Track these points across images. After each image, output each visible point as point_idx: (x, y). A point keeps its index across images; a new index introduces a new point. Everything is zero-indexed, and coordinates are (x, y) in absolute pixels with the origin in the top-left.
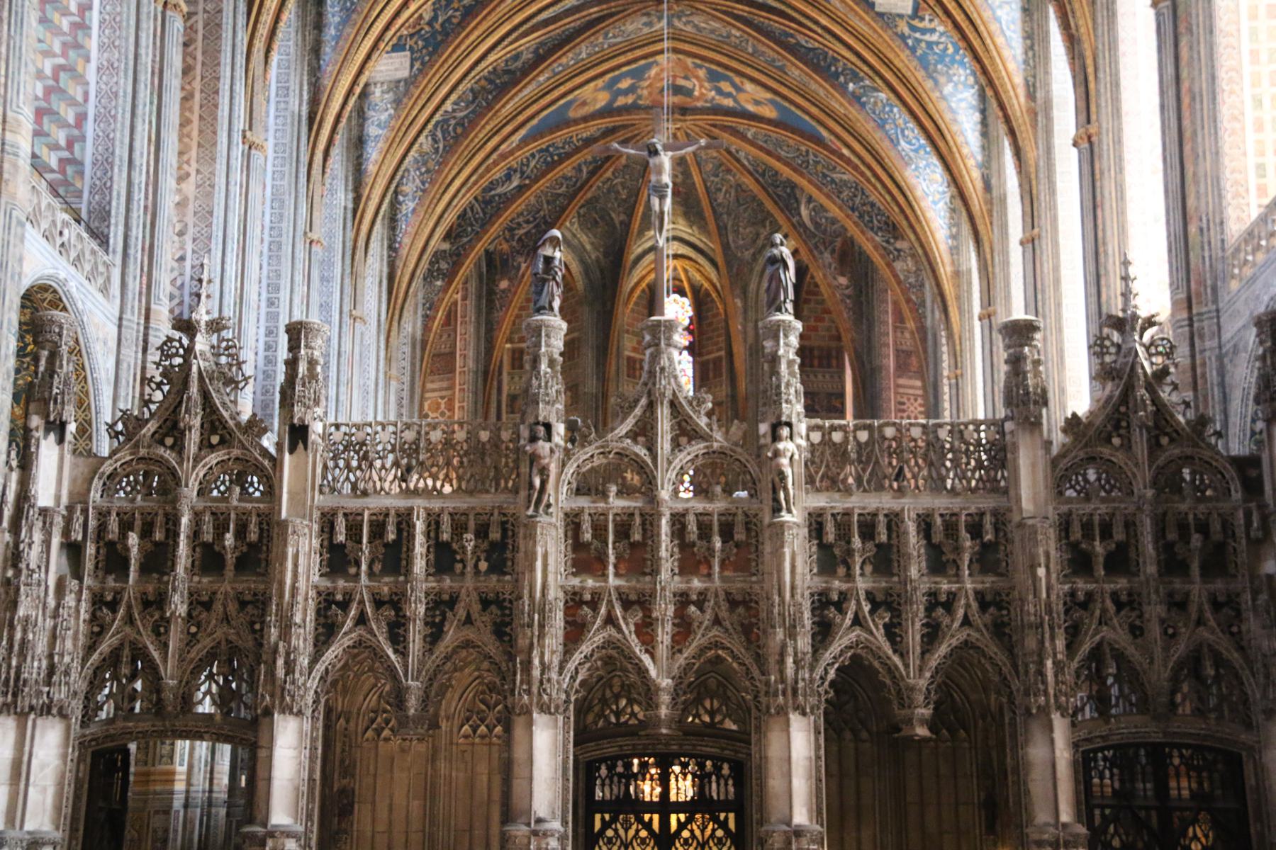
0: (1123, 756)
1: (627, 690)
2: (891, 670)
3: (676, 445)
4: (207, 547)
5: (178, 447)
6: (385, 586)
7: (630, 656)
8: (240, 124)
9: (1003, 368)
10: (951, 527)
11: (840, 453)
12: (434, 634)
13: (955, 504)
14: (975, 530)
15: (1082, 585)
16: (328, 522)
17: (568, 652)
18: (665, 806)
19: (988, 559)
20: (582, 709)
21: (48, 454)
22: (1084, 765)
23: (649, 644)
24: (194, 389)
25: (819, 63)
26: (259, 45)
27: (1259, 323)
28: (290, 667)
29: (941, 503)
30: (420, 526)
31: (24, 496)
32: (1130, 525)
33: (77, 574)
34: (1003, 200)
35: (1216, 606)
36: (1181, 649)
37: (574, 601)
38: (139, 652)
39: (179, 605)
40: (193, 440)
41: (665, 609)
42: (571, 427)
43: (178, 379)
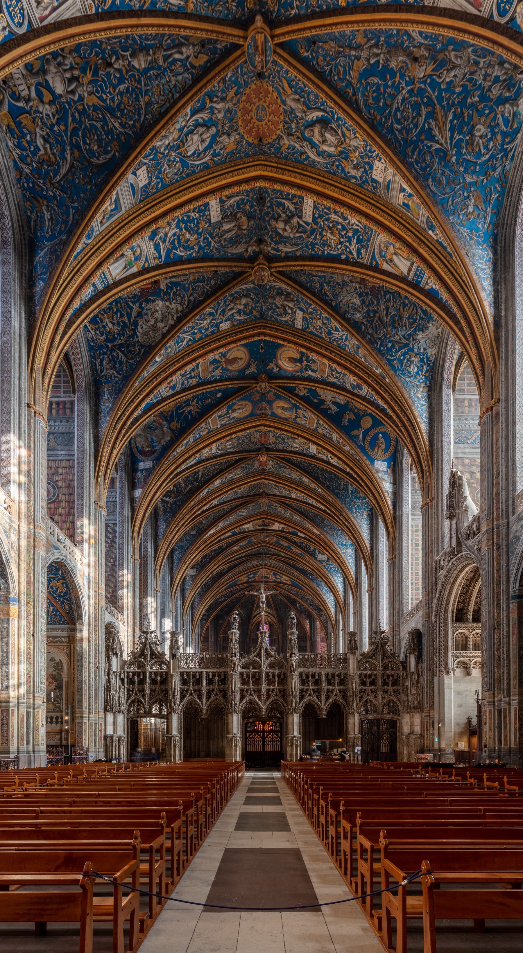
0: (371, 722)
1: (255, 709)
2: (318, 705)
3: (267, 658)
4: (153, 680)
5: (145, 658)
6: (196, 687)
7: (256, 702)
8: (154, 586)
9: (347, 642)
10: (333, 675)
11: (307, 660)
13: (334, 671)
14: (339, 676)
15: (364, 688)
16: (182, 674)
17: (241, 701)
18: (263, 731)
19: (342, 682)
20: (244, 712)
21: (114, 660)
22: (362, 723)
23: (260, 699)
24: (148, 646)
25: (303, 572)
26: (158, 568)
27: (409, 633)
28: (175, 704)
29: (331, 671)
30: (204, 675)
31: (110, 669)
33: (123, 684)
34: (348, 604)
35: (394, 692)
36: (386, 700)
37: (242, 691)
38: (139, 702)
39: (147, 691)
40: (148, 657)
41: (264, 692)
42: (241, 654)
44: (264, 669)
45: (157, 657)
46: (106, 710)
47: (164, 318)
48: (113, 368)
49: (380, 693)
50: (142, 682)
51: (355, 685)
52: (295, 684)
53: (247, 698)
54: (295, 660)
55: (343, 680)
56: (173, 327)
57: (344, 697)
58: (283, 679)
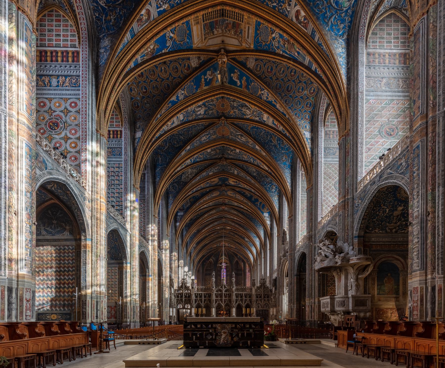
0: (259, 311)
10: (247, 294)
21: (172, 289)
39: (184, 300)
41: (223, 300)
44: (224, 292)
45: (187, 288)
46: (170, 307)
47: (191, 174)
48: (174, 189)
49: (263, 301)
50: (182, 297)
51: (254, 298)
52: (234, 297)
53: (218, 302)
54: (234, 289)
55: (250, 296)
56: (194, 177)
57: (251, 302)
58: (230, 296)
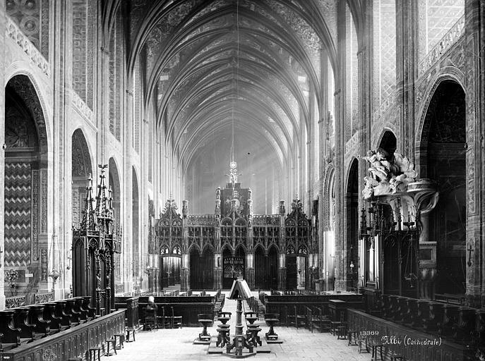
12: (204, 244)
32: (295, 229)
43: (169, 209)
44: (234, 225)
45: (176, 216)
49: (297, 240)
50: (167, 234)
51: (283, 235)
53: (225, 244)
58: (245, 231)
